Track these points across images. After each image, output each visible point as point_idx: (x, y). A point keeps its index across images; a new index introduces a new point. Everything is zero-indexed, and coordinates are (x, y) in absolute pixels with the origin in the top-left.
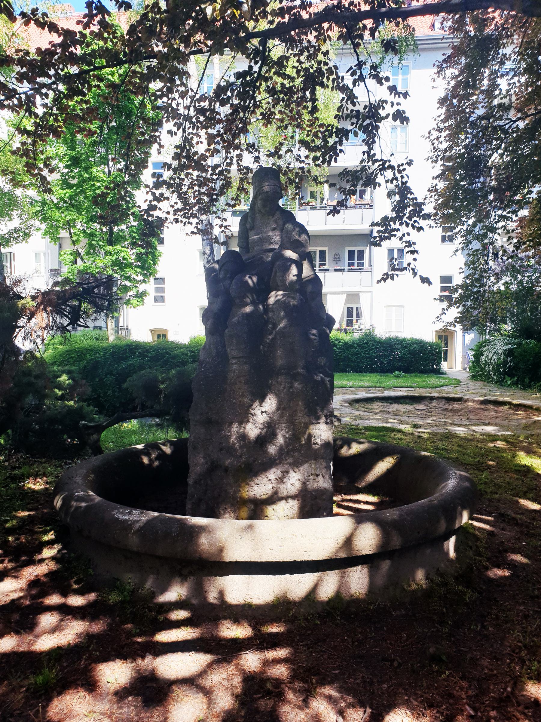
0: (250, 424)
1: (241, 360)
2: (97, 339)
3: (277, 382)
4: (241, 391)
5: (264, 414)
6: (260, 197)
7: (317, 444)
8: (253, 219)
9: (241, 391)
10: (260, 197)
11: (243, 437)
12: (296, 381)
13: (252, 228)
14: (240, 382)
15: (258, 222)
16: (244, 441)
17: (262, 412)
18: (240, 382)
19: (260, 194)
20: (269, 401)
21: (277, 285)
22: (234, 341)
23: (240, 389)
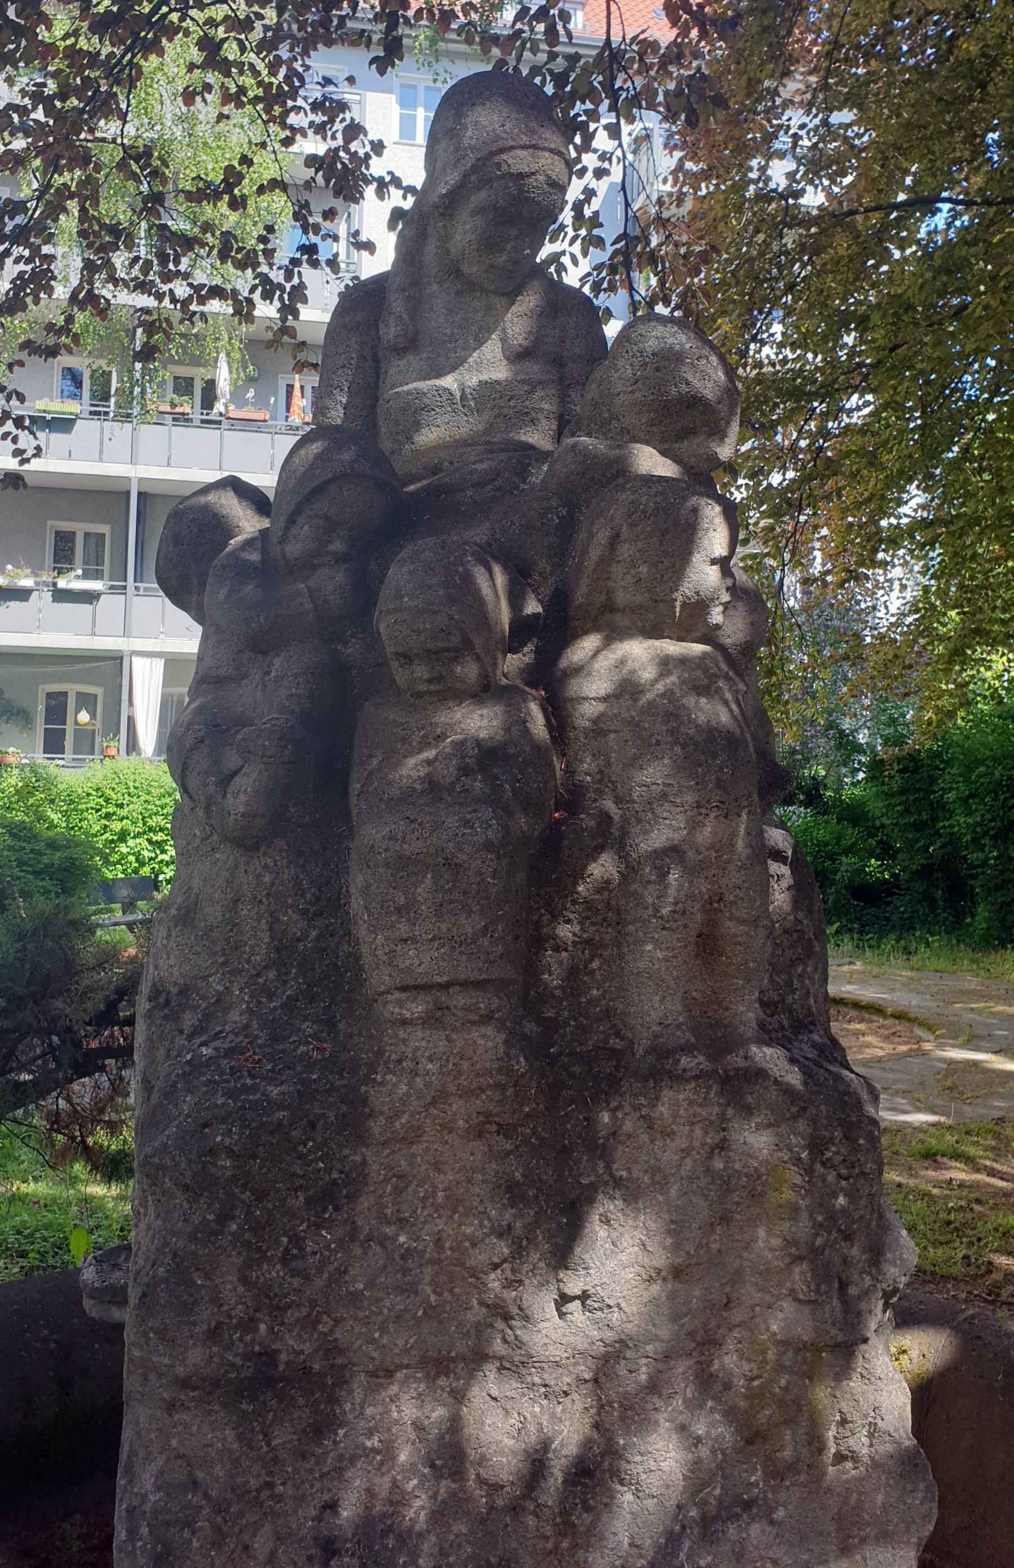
0: (490, 1370)
1: (459, 999)
2: (844, 1422)
3: (649, 1124)
4: (443, 1180)
5: (575, 1306)
6: (481, 197)
7: (855, 1458)
8: (416, 304)
9: (443, 1180)
10: (481, 197)
11: (450, 1454)
12: (748, 1111)
13: (410, 344)
14: (448, 1127)
15: (438, 319)
16: (458, 1474)
17: (564, 1299)
18: (448, 1127)
19: (485, 182)
20: (602, 1232)
21: (610, 607)
22: (422, 891)
23: (437, 1166)
